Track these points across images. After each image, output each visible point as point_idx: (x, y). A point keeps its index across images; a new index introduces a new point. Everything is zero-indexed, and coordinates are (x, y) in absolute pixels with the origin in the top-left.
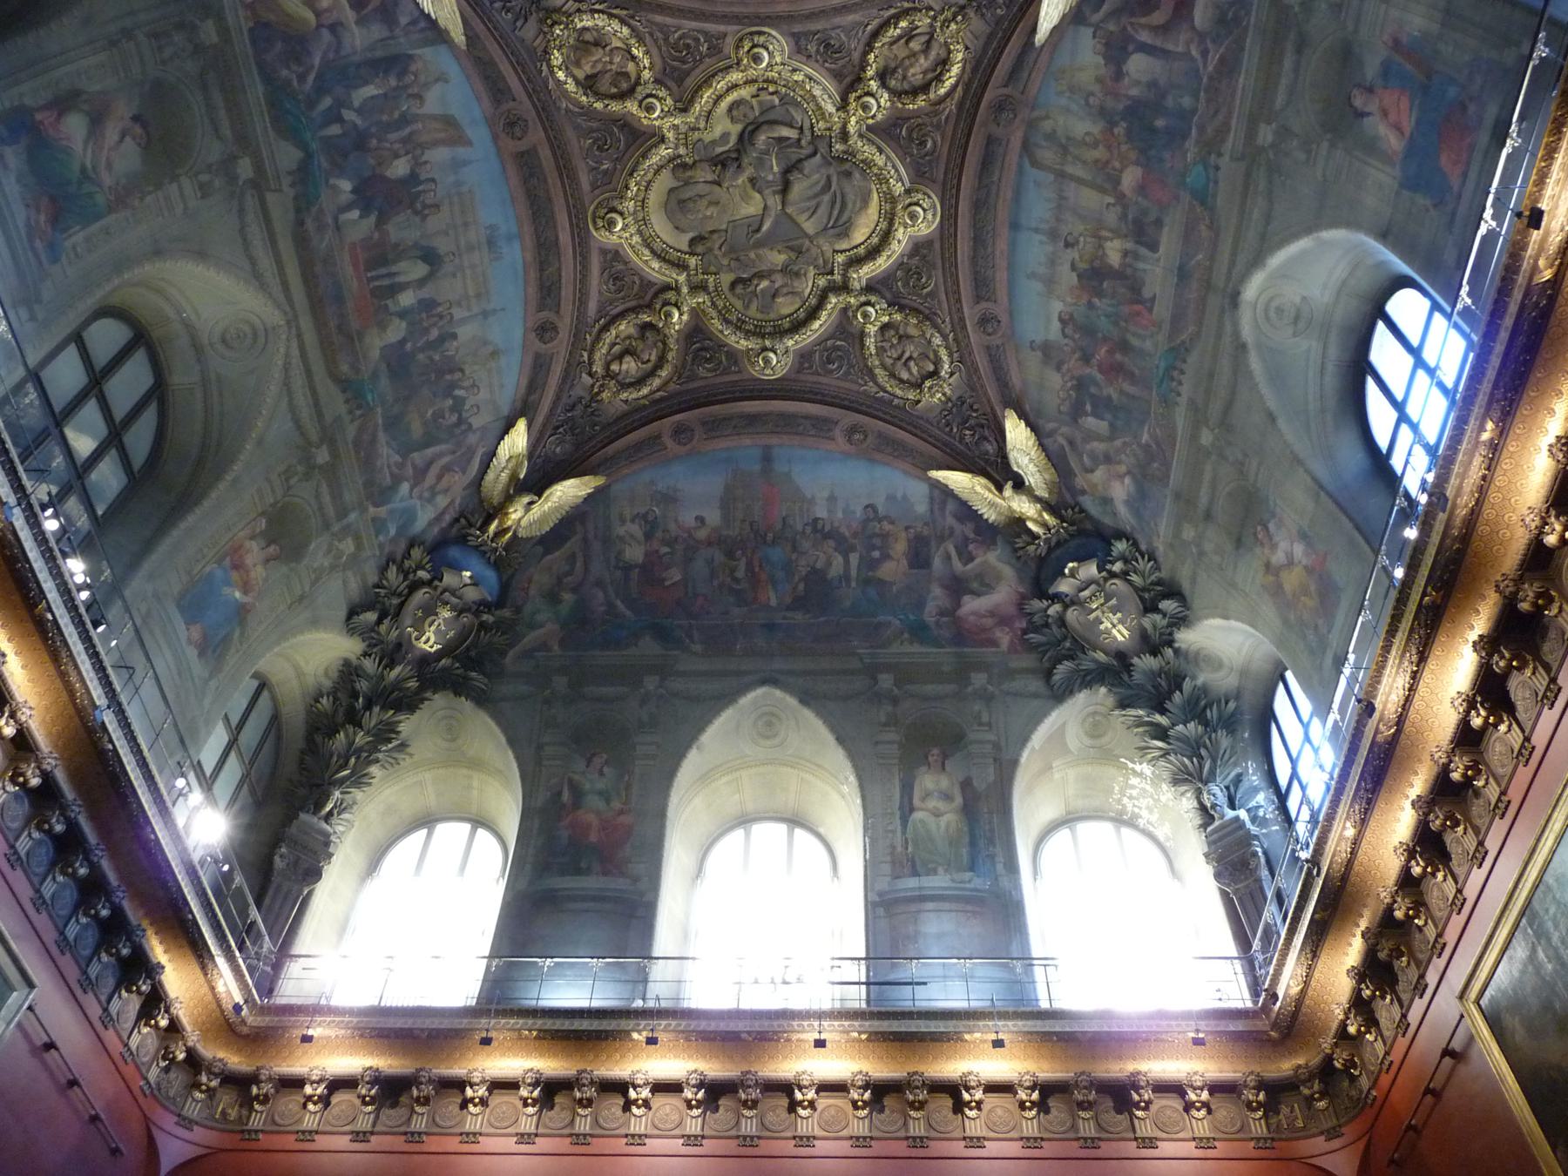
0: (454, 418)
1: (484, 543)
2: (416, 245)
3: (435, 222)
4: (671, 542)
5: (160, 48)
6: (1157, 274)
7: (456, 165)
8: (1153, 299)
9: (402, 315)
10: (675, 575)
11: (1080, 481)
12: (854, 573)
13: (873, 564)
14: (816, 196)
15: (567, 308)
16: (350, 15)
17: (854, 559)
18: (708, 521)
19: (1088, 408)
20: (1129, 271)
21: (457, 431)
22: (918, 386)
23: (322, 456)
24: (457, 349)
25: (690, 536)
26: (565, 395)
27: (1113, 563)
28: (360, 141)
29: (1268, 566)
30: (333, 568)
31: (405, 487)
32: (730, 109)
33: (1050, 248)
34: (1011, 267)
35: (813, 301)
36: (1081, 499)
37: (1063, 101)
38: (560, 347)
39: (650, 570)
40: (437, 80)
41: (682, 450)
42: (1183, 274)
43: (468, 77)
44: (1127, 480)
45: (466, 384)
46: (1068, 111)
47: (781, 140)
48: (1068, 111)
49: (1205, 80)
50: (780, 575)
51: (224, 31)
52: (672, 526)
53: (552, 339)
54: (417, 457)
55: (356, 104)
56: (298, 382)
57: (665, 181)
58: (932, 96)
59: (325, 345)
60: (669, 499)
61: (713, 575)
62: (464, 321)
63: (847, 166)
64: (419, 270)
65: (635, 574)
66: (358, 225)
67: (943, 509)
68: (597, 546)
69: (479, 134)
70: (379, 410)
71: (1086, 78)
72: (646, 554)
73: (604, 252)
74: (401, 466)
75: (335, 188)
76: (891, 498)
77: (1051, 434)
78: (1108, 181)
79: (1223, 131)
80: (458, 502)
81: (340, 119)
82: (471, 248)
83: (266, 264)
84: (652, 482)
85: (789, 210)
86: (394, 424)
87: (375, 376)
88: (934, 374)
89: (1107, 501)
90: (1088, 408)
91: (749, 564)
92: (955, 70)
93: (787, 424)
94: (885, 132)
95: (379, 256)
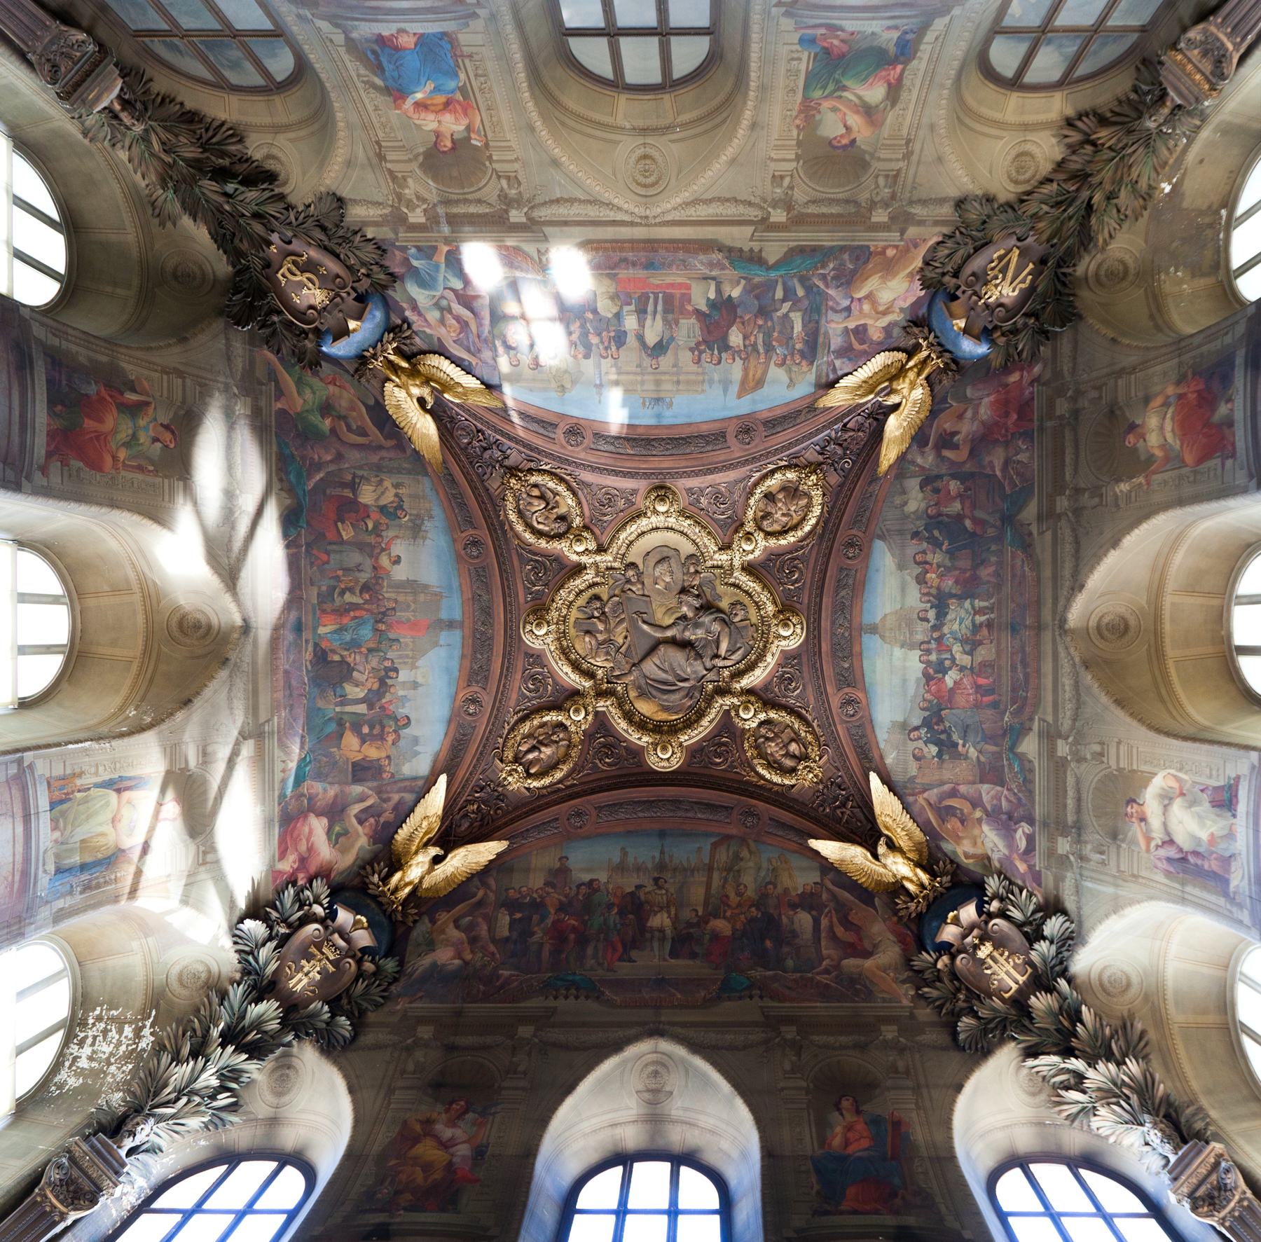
4: (377, 531)
5: (887, 176)
10: (347, 533)
14: (673, 669)
15: (592, 458)
18: (396, 566)
25: (383, 550)
35: (585, 666)
37: (765, 865)
39: (349, 508)
40: (791, 380)
41: (460, 547)
48: (759, 869)
49: (810, 975)
52: (391, 533)
55: (792, 315)
57: (687, 548)
58: (756, 761)
60: (416, 531)
61: (347, 570)
63: (697, 695)
65: (348, 493)
69: (743, 406)
71: (785, 881)
72: (366, 506)
79: (774, 996)
81: (784, 300)
84: (431, 517)
85: (662, 648)
92: (777, 779)
94: (727, 724)
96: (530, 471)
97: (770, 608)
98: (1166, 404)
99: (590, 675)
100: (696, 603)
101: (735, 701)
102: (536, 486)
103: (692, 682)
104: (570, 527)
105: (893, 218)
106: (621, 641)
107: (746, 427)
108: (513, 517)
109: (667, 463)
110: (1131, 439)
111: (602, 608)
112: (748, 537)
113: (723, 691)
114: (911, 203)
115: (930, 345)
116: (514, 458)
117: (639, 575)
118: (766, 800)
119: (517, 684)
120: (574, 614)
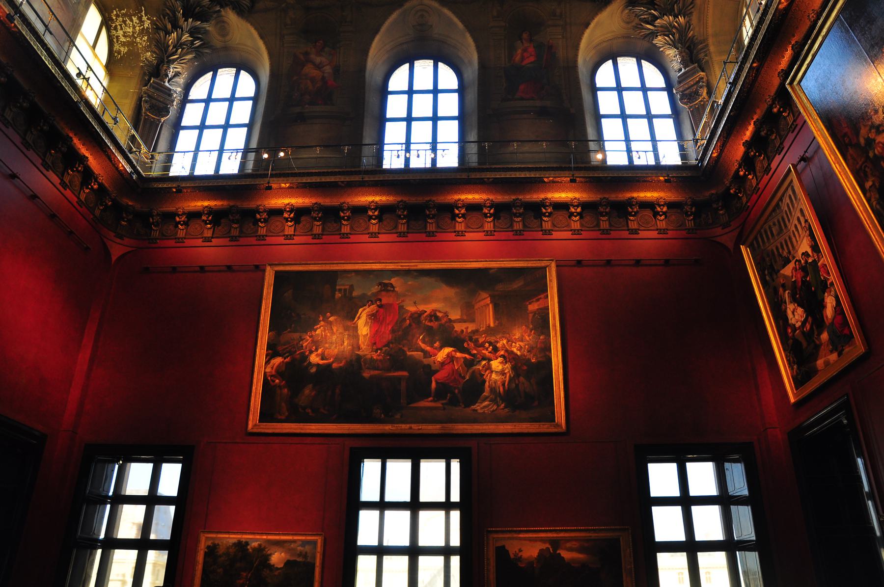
29: (307, 54)
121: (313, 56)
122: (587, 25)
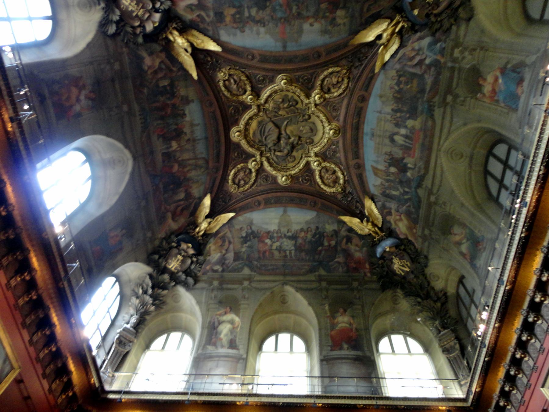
0: (401, 79)
1: (404, 21)
2: (396, 146)
3: (387, 149)
4: (324, 17)
6: (159, 146)
7: (377, 162)
8: (158, 139)
9: (406, 127)
10: (324, 6)
11: (163, 55)
12: (246, 10)
13: (238, 13)
14: (269, 135)
16: (393, 211)
17: (246, 14)
19: (168, 88)
20: (168, 142)
21: (402, 73)
22: (230, 75)
23: (449, 98)
24: (393, 105)
26: (360, 72)
27: (140, 32)
28: (401, 182)
29: (84, 86)
30: (466, 49)
31: (427, 61)
32: (295, 160)
33: (195, 135)
34: (205, 124)
35: (270, 99)
36: (161, 48)
37: (200, 177)
38: (358, 93)
42: (152, 153)
43: (367, 183)
44: (146, 68)
45: (393, 90)
46: (198, 176)
47: (280, 151)
50: (277, 8)
51: (423, 230)
53: (360, 96)
54: (417, 71)
56: (445, 130)
57: (316, 139)
59: (432, 136)
60: (325, 32)
61: (307, 6)
62: (388, 114)
63: (260, 144)
64: (396, 138)
65: (341, 5)
66: (409, 162)
67: (213, 31)
68: (357, 14)
70: (425, 98)
71: (194, 186)
72: (335, 12)
73: (338, 120)
74: (425, 72)
75: (412, 176)
76: (235, 35)
77: (179, 70)
78: (182, 164)
80: (411, 41)
81: (404, 191)
82: (379, 136)
83: (438, 172)
84: (330, 38)
85: (277, 130)
86: (422, 91)
87: (422, 112)
88: (224, 81)
89: (151, 54)
90: (168, 88)
91: (291, 10)
92: (230, 177)
93: (276, 59)
94: (250, 156)
95: (407, 149)
96: (349, 78)
97: (293, 172)
98: (351, 324)
99: (266, 101)
100: (295, 143)
101: (258, 160)
102: (343, 80)
103: (265, 142)
104: (325, 93)
105: (425, 236)
106: (280, 113)
107: (360, 167)
108: (330, 70)
109: (349, 135)
110: (341, 310)
111: (294, 106)
112: (319, 164)
113: (261, 155)
114: (429, 243)
115: (382, 236)
116: (355, 72)
117: (306, 120)
118: (223, 174)
119: (260, 73)
120: (290, 94)
121: (84, 92)
122: (136, 261)
